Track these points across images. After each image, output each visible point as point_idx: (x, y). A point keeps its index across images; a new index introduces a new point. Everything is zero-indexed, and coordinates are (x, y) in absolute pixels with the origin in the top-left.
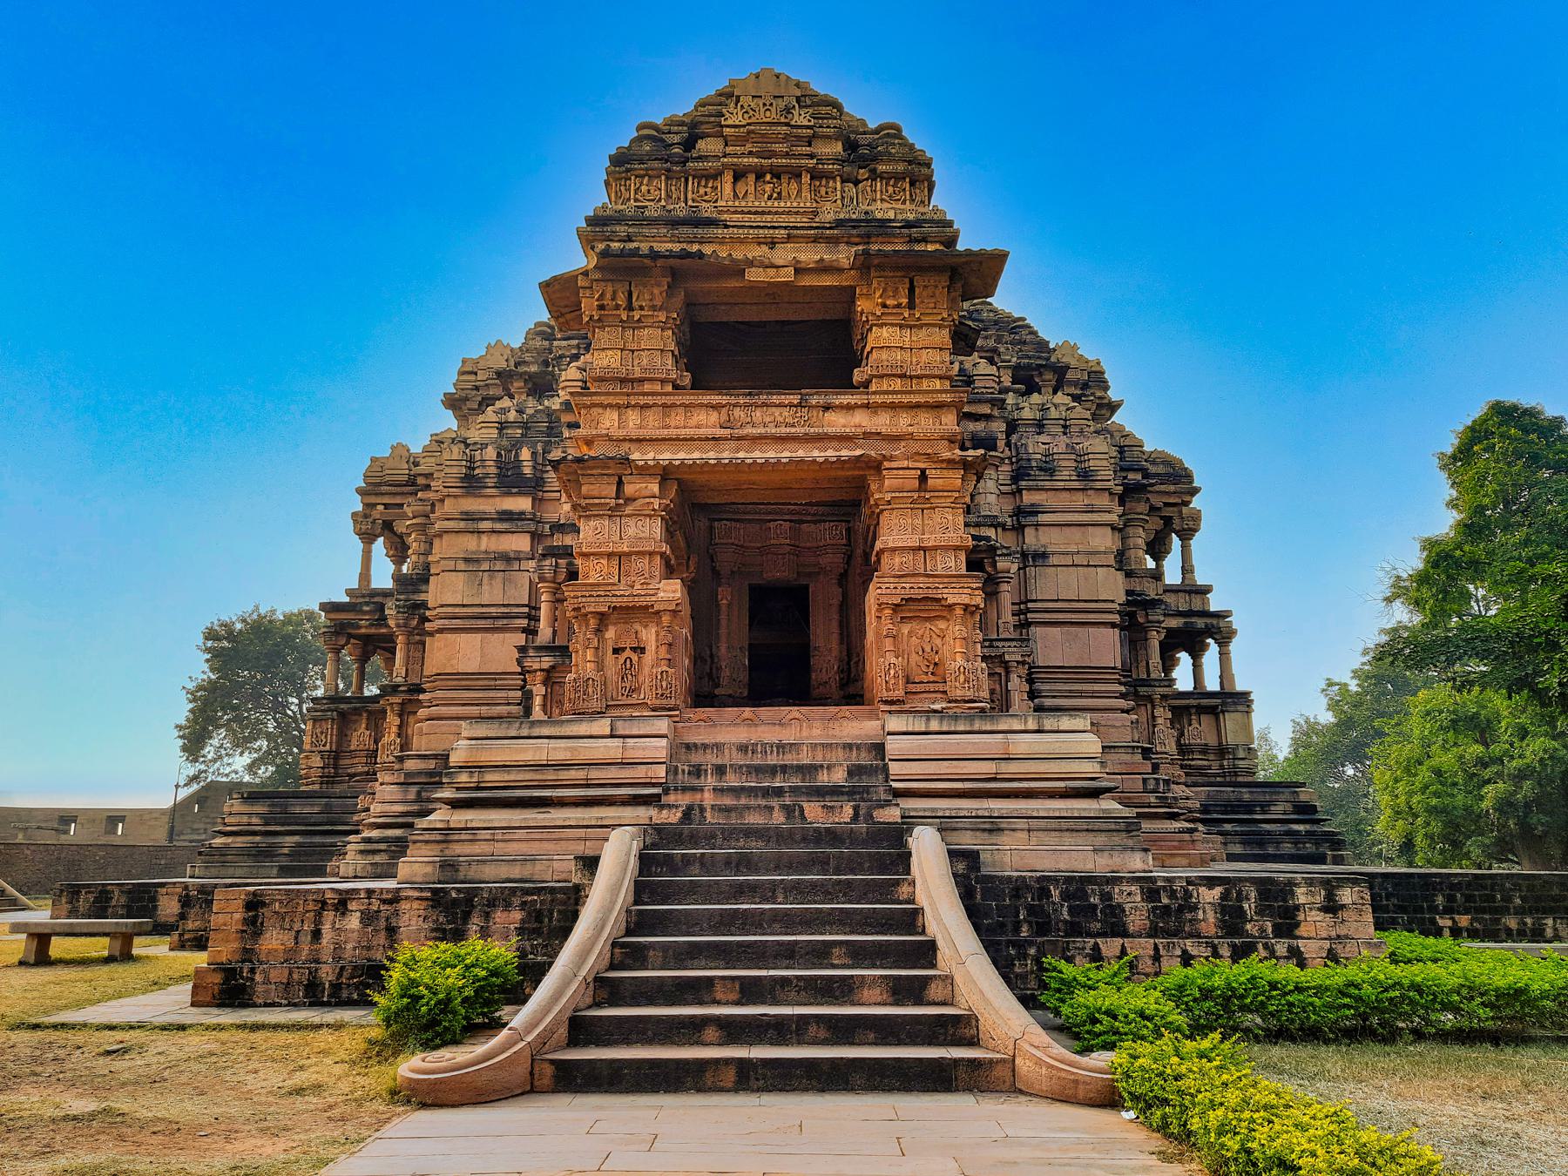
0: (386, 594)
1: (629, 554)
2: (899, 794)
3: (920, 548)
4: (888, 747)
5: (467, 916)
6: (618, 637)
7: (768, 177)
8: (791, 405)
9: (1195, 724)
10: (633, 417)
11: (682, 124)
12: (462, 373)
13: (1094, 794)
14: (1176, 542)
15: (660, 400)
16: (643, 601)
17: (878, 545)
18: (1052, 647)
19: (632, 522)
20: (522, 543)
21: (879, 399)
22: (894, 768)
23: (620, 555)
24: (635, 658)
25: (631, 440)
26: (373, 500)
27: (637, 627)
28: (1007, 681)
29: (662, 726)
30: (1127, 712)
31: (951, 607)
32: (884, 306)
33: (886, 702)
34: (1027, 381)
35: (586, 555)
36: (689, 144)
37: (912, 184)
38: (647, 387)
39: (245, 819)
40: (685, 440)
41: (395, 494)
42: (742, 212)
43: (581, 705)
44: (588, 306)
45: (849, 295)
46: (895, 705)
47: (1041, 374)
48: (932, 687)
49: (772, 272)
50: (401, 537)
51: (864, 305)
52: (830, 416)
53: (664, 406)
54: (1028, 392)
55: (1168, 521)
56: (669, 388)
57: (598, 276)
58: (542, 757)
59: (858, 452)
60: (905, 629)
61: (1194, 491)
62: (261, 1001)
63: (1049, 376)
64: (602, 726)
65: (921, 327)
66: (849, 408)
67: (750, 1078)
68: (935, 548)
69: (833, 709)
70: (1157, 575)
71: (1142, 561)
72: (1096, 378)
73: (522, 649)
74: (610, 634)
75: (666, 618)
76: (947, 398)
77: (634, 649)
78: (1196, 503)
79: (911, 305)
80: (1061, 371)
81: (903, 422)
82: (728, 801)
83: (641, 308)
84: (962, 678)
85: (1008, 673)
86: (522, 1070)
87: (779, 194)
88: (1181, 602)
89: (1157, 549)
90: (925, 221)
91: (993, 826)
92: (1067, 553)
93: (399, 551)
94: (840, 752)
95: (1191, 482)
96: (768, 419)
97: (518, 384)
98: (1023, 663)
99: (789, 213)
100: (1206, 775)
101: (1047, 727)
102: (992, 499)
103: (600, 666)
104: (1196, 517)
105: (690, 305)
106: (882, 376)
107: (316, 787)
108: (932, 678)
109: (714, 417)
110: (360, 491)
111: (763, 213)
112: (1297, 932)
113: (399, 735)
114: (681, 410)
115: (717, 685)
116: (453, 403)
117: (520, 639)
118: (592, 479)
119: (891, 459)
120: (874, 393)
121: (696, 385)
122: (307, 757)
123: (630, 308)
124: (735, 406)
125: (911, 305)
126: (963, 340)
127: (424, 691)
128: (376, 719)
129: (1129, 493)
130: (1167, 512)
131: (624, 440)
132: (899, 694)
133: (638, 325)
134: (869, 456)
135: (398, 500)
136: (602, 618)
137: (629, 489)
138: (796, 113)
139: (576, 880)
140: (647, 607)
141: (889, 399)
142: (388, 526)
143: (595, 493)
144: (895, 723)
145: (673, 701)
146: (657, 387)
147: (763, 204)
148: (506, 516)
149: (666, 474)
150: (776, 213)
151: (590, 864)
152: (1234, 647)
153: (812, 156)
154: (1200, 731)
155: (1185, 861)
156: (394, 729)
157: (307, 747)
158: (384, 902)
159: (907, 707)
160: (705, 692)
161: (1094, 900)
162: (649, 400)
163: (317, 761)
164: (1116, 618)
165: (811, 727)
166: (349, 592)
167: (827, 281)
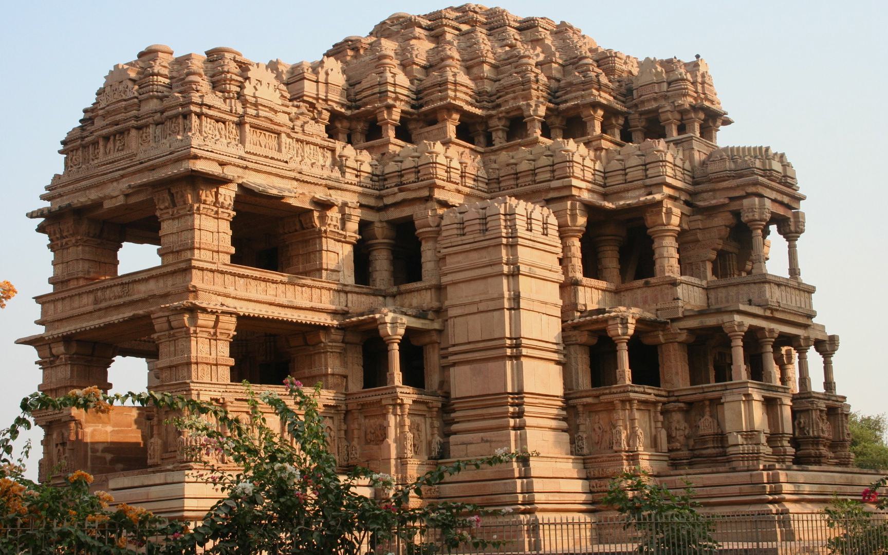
8: (118, 285)
10: (60, 305)
19: (59, 369)
38: (72, 284)
45: (150, 204)
56: (82, 282)
59: (131, 314)
74: (55, 436)
83: (67, 237)
92: (474, 303)
100: (717, 462)
101: (169, 481)
109: (91, 298)
111: (113, 162)
124: (97, 290)
130: (735, 206)
132: (157, 460)
140: (60, 420)
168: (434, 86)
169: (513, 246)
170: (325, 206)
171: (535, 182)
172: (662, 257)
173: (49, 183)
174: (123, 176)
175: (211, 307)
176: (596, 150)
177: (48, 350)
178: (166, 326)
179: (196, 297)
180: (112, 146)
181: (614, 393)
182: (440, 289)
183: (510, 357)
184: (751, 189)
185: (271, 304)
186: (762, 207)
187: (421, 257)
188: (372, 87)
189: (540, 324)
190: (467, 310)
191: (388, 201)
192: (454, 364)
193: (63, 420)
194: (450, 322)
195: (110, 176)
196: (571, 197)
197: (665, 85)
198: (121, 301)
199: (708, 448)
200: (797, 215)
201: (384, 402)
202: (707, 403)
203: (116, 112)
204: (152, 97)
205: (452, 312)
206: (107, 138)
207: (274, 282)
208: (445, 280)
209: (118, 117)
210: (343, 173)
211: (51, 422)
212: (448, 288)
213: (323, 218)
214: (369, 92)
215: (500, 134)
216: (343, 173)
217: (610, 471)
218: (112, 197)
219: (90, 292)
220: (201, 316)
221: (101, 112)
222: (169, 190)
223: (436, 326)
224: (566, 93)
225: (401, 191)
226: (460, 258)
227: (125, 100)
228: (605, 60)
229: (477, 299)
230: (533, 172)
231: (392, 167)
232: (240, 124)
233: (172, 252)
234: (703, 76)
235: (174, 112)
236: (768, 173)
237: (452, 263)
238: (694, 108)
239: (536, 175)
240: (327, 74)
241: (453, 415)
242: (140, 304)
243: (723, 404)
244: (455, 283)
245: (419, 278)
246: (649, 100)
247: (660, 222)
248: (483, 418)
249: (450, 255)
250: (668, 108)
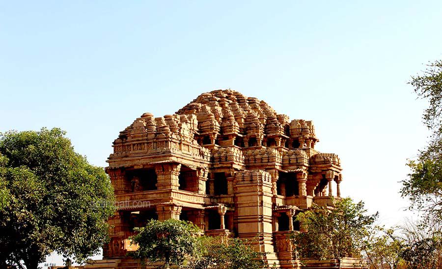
19: (115, 220)
21: (158, 192)
58: (99, 266)
66: (153, 194)
74: (113, 242)
79: (163, 171)
168: (227, 126)
169: (261, 186)
170: (199, 169)
171: (262, 162)
172: (301, 189)
175: (177, 205)
176: (280, 151)
178: (162, 209)
179: (172, 201)
182: (235, 198)
183: (259, 222)
184: (330, 168)
185: (188, 202)
186: (333, 174)
187: (227, 186)
188: (208, 126)
189: (268, 212)
190: (245, 205)
191: (215, 166)
192: (240, 222)
194: (239, 209)
195: (137, 158)
196: (275, 168)
200: (340, 175)
204: (152, 133)
205: (239, 206)
206: (134, 145)
207: (189, 195)
208: (237, 195)
210: (203, 157)
213: (199, 173)
214: (207, 127)
215: (247, 143)
216: (203, 157)
217: (287, 258)
219: (129, 196)
220: (175, 207)
223: (233, 210)
224: (269, 130)
225: (220, 163)
226: (242, 188)
228: (280, 118)
229: (249, 202)
230: (262, 159)
231: (216, 155)
232: (180, 144)
234: (312, 127)
235: (163, 140)
236: (334, 163)
238: (310, 138)
240: (193, 121)
244: (240, 196)
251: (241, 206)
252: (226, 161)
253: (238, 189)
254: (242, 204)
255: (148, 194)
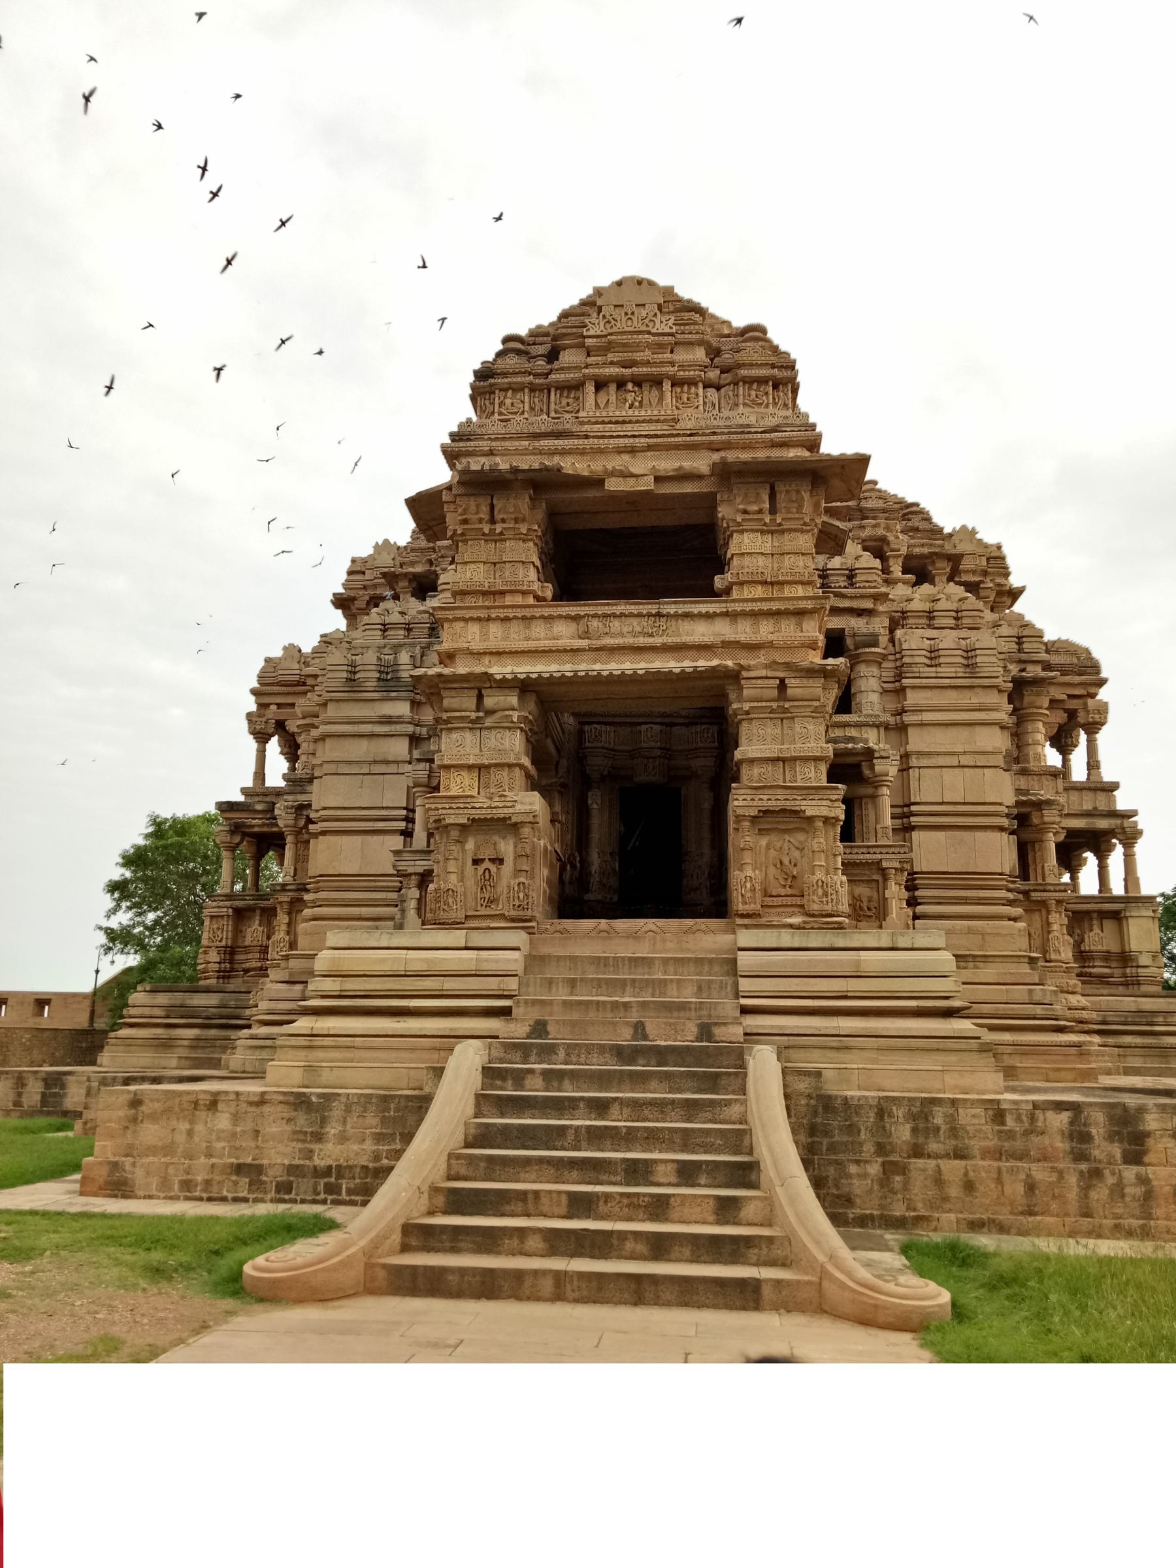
0: (278, 793)
1: (488, 767)
2: (745, 1011)
3: (778, 759)
4: (739, 962)
5: (324, 1121)
6: (477, 848)
7: (630, 386)
8: (649, 615)
9: (1096, 930)
10: (495, 629)
11: (547, 335)
12: (350, 573)
13: (949, 1013)
14: (1083, 737)
15: (519, 613)
16: (501, 813)
17: (738, 755)
18: (932, 851)
20: (400, 748)
21: (738, 607)
22: (745, 985)
23: (481, 769)
24: (493, 868)
25: (491, 653)
26: (266, 700)
27: (496, 838)
28: (885, 888)
29: (518, 938)
30: (1015, 919)
31: (811, 819)
32: (745, 512)
33: (743, 916)
34: (919, 571)
35: (448, 767)
36: (552, 356)
37: (775, 387)
38: (509, 600)
39: (147, 1011)
40: (544, 651)
41: (289, 694)
42: (603, 423)
43: (442, 915)
44: (452, 521)
45: (709, 502)
46: (753, 919)
47: (933, 563)
48: (789, 901)
49: (632, 481)
50: (293, 735)
51: (724, 511)
52: (685, 626)
53: (524, 618)
54: (918, 583)
55: (1072, 714)
56: (531, 600)
57: (461, 491)
59: (715, 662)
60: (763, 841)
61: (1102, 682)
62: (142, 1193)
63: (941, 564)
64: (457, 937)
65: (782, 532)
66: (709, 616)
67: (562, 1289)
68: (794, 759)
69: (689, 922)
70: (1064, 772)
71: (1039, 757)
72: (996, 561)
73: (397, 853)
74: (470, 845)
75: (526, 831)
76: (809, 605)
77: (492, 860)
78: (1103, 694)
79: (773, 511)
80: (955, 560)
81: (765, 631)
82: (575, 1016)
83: (503, 521)
84: (820, 891)
85: (886, 879)
86: (356, 1273)
87: (641, 402)
88: (1087, 802)
89: (1062, 741)
90: (787, 425)
91: (842, 1043)
93: (291, 751)
94: (692, 968)
95: (1098, 672)
96: (625, 630)
97: (403, 584)
98: (902, 870)
99: (650, 421)
100: (1108, 983)
101: (900, 945)
102: (874, 697)
103: (462, 879)
104: (1103, 709)
105: (553, 515)
106: (742, 584)
107: (214, 981)
108: (789, 891)
110: (254, 692)
112: (1146, 1159)
113: (288, 933)
114: (540, 622)
115: (588, 891)
116: (340, 602)
117: (397, 842)
118: (453, 693)
119: (749, 668)
120: (734, 601)
121: (557, 597)
122: (205, 953)
123: (493, 521)
124: (594, 616)
125: (773, 511)
126: (830, 542)
127: (307, 891)
128: (269, 914)
129: (1019, 689)
130: (1073, 704)
131: (485, 653)
133: (500, 538)
134: (726, 667)
135: (290, 700)
136: (463, 828)
137: (489, 702)
138: (657, 321)
139: (427, 1090)
140: (505, 819)
141: (748, 607)
142: (280, 726)
143: (455, 706)
144: (746, 938)
145: (529, 913)
146: (519, 600)
147: (625, 413)
148: (388, 720)
149: (524, 687)
150: (637, 422)
151: (438, 1072)
152: (1140, 848)
153: (672, 364)
154: (1100, 939)
155: (1070, 1076)
156: (284, 927)
157: (204, 942)
158: (251, 1104)
159: (763, 920)
160: (572, 902)
161: (938, 1120)
162: (510, 613)
163: (213, 956)
164: (1005, 822)
165: (664, 941)
166: (244, 791)
167: (688, 488)
173: (455, 429)
174: (650, 448)
177: (475, 701)
178: (776, 692)
180: (613, 398)
181: (1050, 891)
190: (941, 761)
193: (514, 819)
195: (622, 442)
197: (984, 559)
198: (658, 641)
199: (1094, 967)
201: (884, 864)
202: (1095, 915)
203: (636, 348)
205: (914, 762)
208: (908, 718)
209: (638, 356)
211: (474, 820)
212: (910, 730)
218: (633, 475)
219: (576, 618)
221: (589, 341)
222: (772, 488)
227: (649, 333)
233: (764, 583)
237: (913, 698)
239: (931, 618)
241: (917, 893)
242: (693, 653)
243: (1127, 918)
244: (922, 725)
245: (849, 711)
246: (967, 572)
247: (1038, 704)
248: (965, 901)
249: (913, 687)
250: (991, 585)
251: (925, 762)
252: (852, 585)
253: (910, 694)
254: (929, 754)
255: (687, 616)
